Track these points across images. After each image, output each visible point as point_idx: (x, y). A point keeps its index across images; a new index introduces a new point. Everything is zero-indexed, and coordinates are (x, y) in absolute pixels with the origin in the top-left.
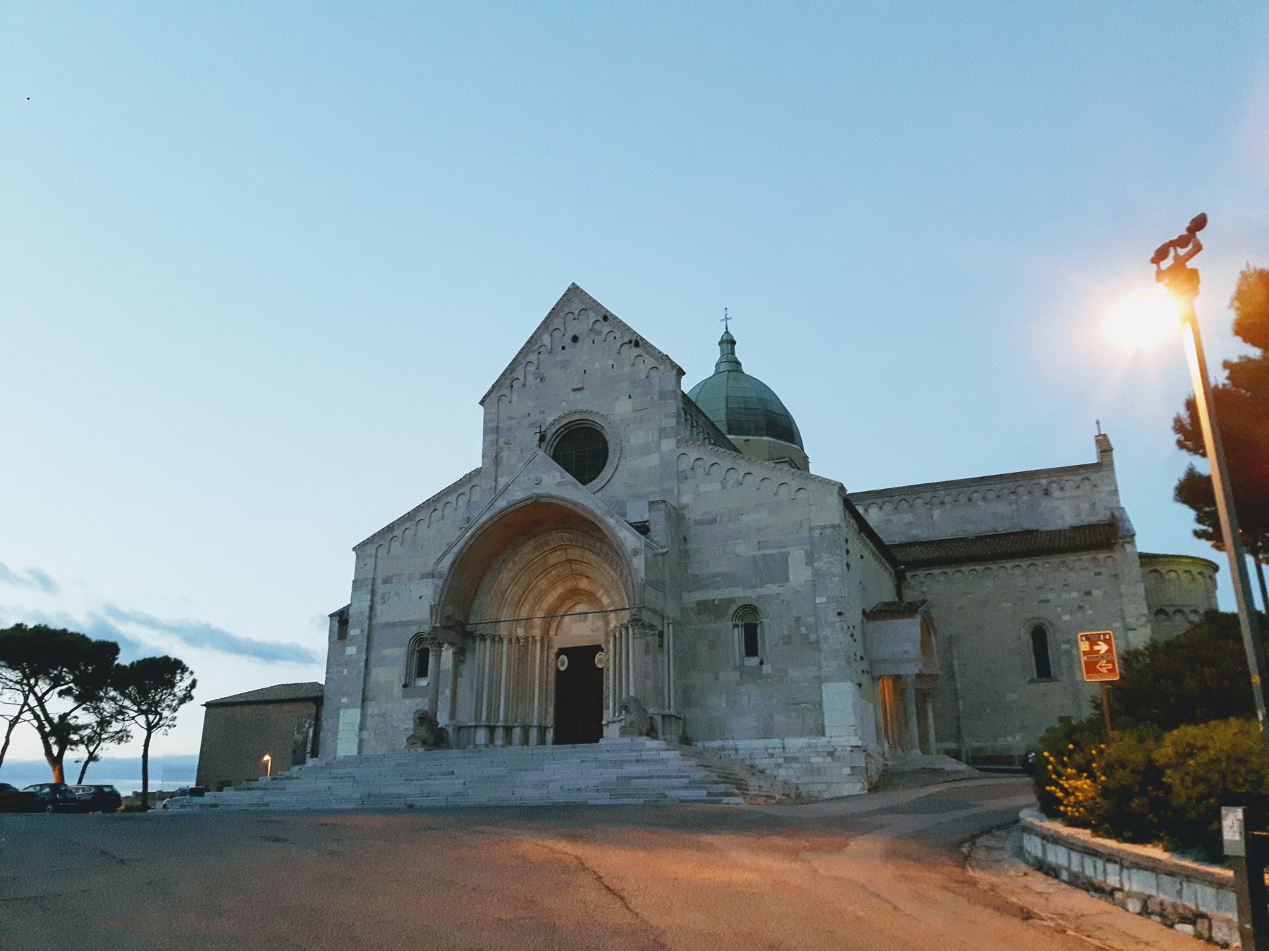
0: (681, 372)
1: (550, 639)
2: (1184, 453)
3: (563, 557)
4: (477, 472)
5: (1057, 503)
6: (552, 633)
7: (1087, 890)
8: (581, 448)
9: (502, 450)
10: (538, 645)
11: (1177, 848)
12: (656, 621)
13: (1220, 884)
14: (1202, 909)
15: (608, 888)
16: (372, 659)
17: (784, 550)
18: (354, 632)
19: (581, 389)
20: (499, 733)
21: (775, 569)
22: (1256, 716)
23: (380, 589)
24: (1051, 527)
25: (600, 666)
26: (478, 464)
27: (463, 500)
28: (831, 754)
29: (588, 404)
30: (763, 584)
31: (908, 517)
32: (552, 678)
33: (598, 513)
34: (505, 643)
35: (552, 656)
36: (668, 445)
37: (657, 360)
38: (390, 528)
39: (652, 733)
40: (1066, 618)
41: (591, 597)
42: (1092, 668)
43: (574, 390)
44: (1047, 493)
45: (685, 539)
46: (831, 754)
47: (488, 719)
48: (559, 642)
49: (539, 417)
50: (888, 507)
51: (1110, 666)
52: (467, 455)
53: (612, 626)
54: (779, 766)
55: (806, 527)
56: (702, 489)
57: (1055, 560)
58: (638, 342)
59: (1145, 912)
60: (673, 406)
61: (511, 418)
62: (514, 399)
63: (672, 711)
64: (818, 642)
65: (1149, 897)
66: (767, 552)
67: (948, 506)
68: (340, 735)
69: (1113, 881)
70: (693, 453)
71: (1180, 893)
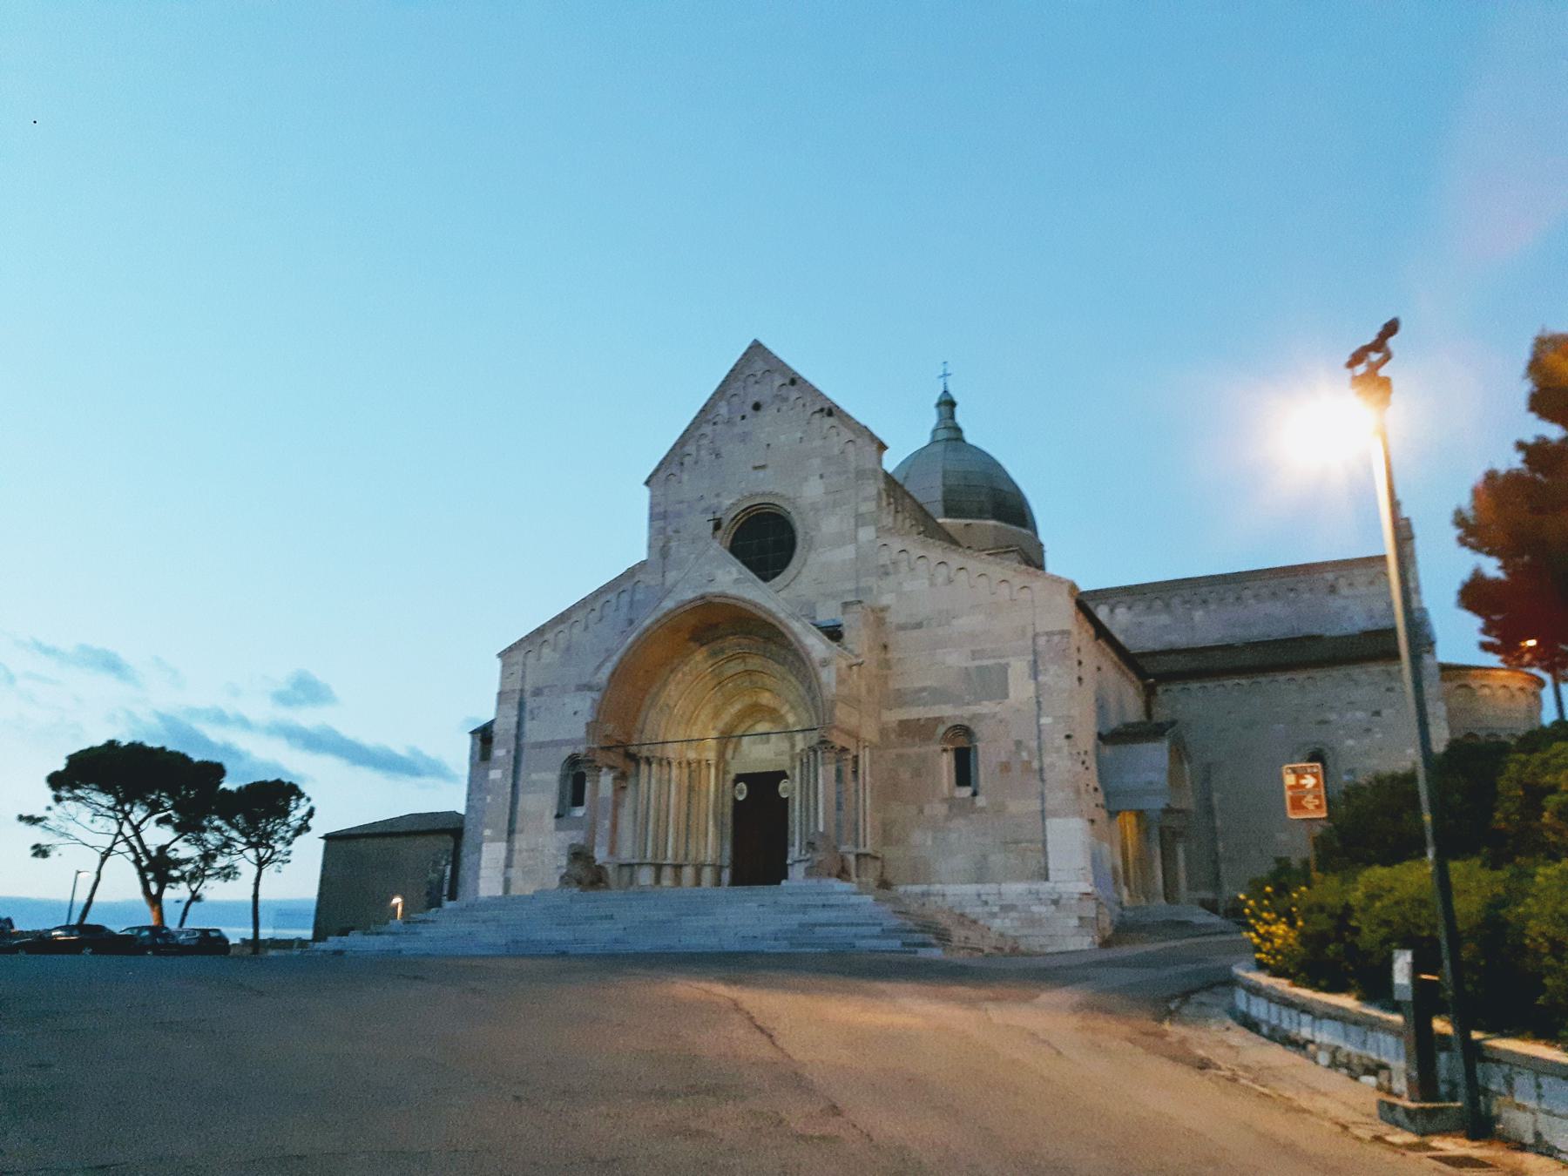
0: (882, 447)
1: (726, 763)
2: (1466, 551)
3: (741, 668)
4: (643, 564)
5: (1341, 602)
6: (729, 755)
7: (1283, 1044)
8: (765, 539)
9: (668, 540)
10: (713, 770)
11: (1367, 997)
12: (850, 744)
13: (1388, 1028)
14: (1384, 1060)
15: (758, 1027)
16: (521, 783)
17: (1002, 661)
18: (499, 752)
19: (763, 467)
20: (668, 873)
21: (992, 682)
22: (1425, 854)
23: (530, 703)
24: (1336, 632)
25: (784, 796)
26: (641, 554)
27: (625, 598)
28: (1056, 902)
29: (769, 486)
30: (978, 701)
31: (1164, 619)
32: (728, 810)
33: (782, 615)
34: (674, 765)
35: (729, 784)
36: (867, 534)
37: (854, 431)
38: (540, 631)
39: (843, 874)
40: (1350, 742)
41: (773, 714)
42: (1297, 804)
43: (756, 468)
44: (1333, 589)
45: (885, 647)
46: (1056, 902)
47: (655, 856)
48: (736, 768)
49: (715, 501)
50: (1140, 606)
51: (1317, 802)
52: (632, 546)
53: (798, 750)
54: (994, 915)
55: (1030, 634)
56: (907, 587)
57: (1338, 673)
58: (831, 411)
59: (1334, 1064)
60: (873, 487)
62: (685, 477)
63: (868, 850)
64: (1041, 770)
65: (1338, 1048)
66: (985, 662)
67: (1213, 607)
68: (483, 873)
69: (1306, 1033)
70: (896, 544)
71: (1364, 1043)
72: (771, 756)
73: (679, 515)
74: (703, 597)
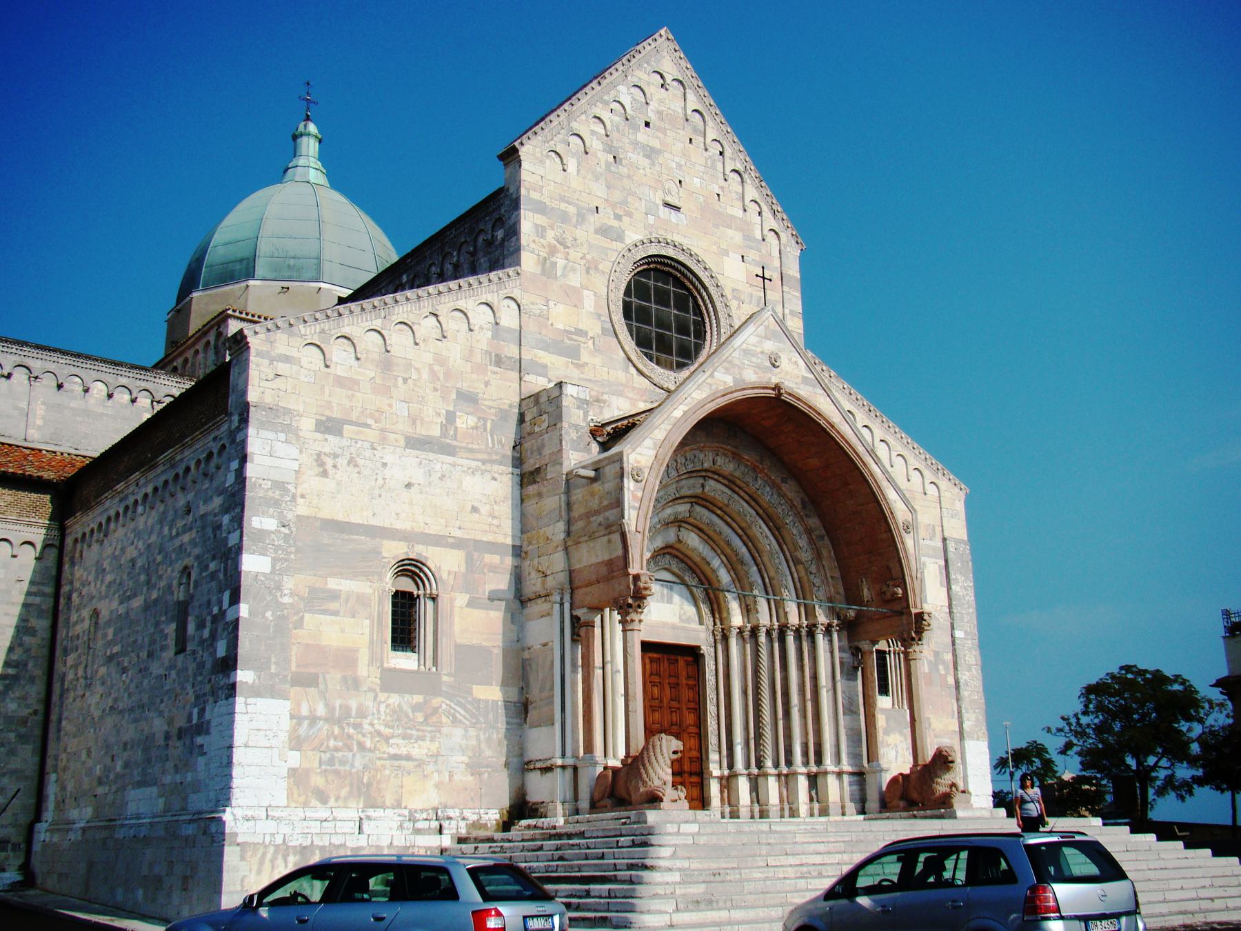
9: (553, 251)
19: (677, 208)
43: (667, 205)
61: (563, 199)
72: (675, 620)
73: (564, 218)
74: (777, 388)
